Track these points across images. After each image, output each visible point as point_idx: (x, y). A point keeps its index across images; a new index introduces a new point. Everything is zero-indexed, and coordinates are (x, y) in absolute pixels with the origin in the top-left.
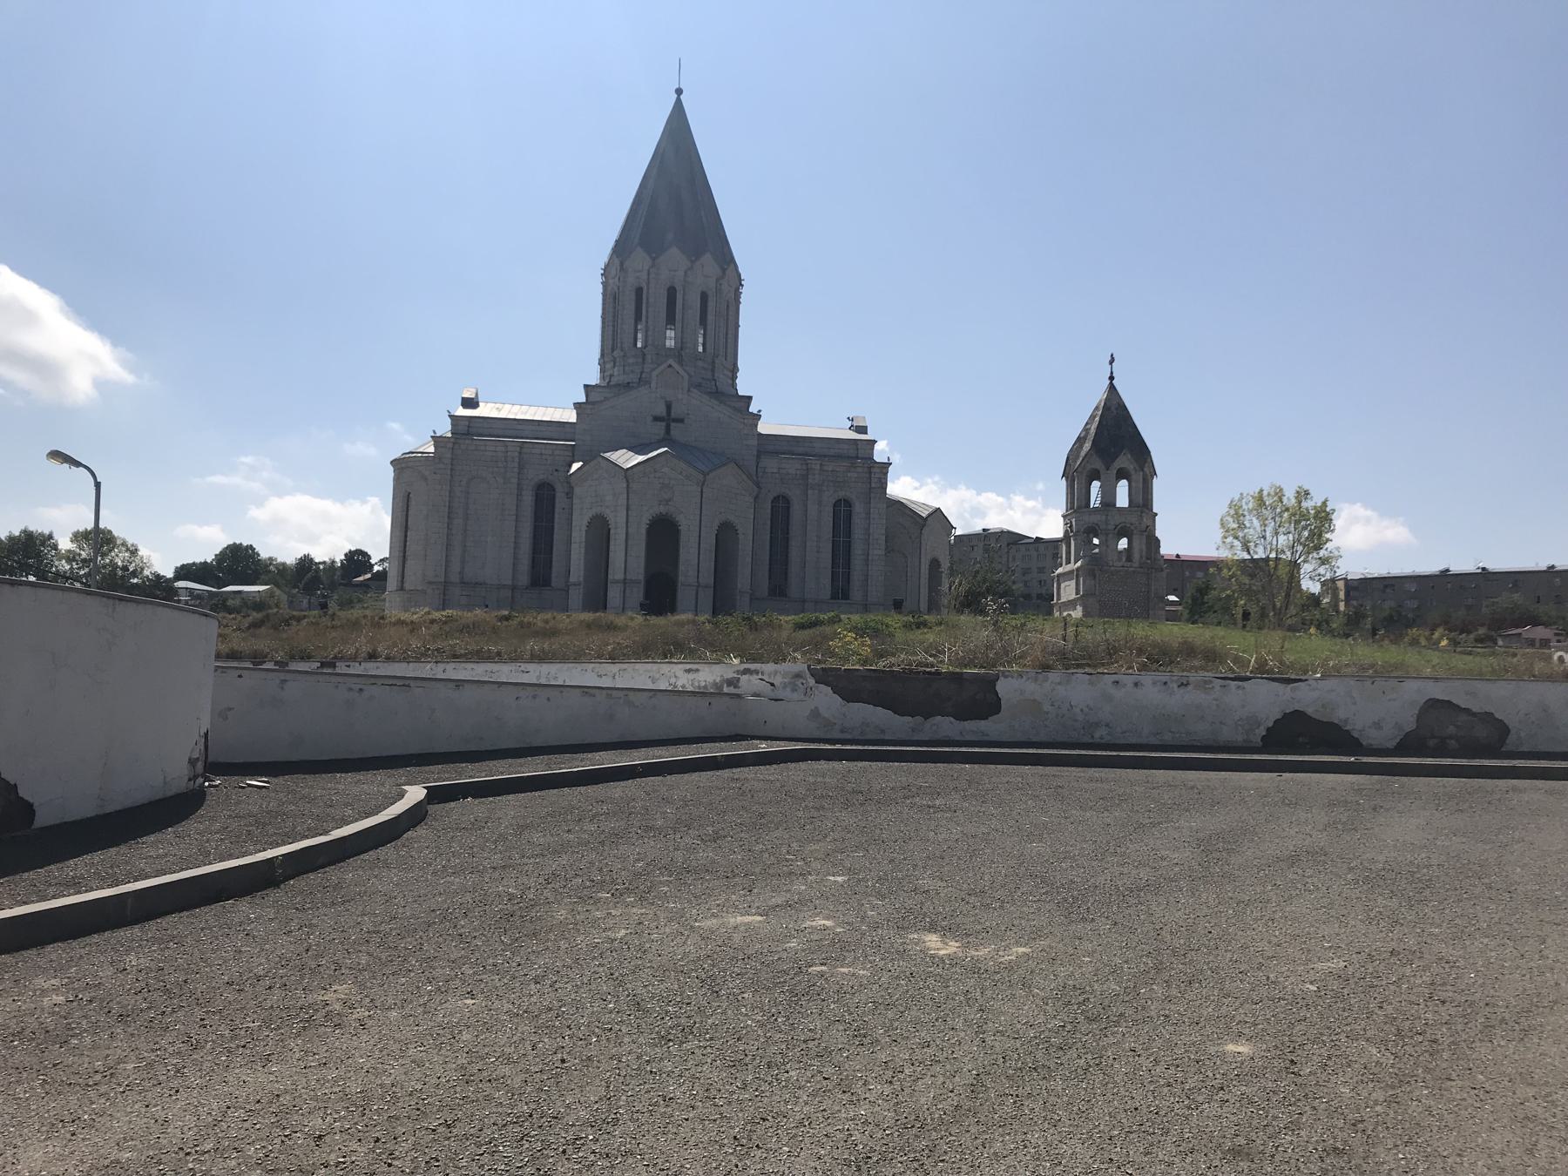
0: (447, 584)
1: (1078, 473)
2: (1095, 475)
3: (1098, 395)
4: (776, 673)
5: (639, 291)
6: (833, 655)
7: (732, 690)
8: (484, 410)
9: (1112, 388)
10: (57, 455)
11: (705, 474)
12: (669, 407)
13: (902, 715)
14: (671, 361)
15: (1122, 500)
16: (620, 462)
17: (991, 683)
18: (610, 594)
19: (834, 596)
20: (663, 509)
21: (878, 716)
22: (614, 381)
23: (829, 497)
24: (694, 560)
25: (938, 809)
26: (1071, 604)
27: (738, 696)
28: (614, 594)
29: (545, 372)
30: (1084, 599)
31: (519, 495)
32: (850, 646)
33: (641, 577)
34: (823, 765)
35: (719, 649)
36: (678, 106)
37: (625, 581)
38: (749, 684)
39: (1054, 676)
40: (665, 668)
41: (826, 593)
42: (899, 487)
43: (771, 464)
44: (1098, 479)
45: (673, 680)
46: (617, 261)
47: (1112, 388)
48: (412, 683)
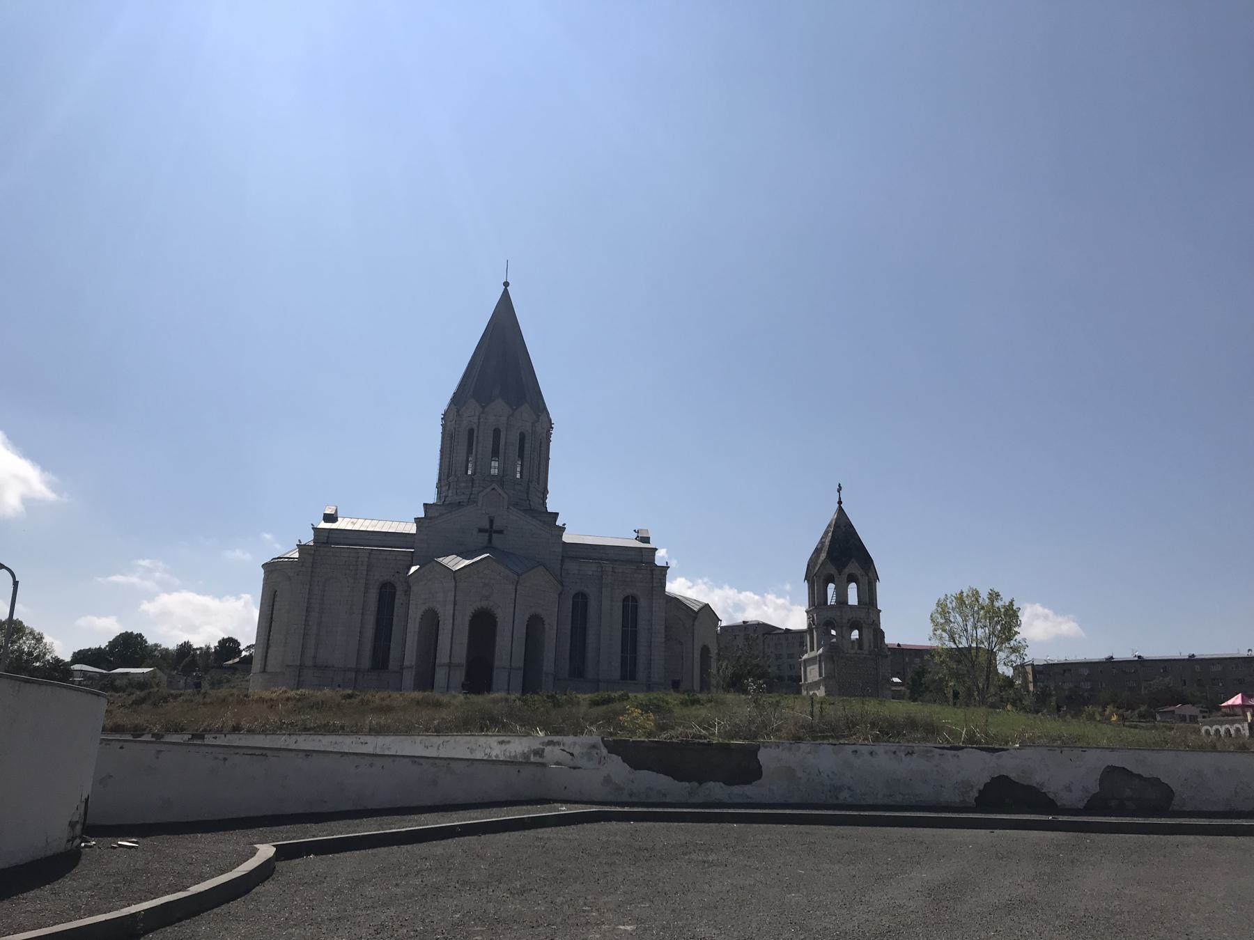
0: (302, 667)
1: (817, 577)
2: (830, 579)
3: (830, 515)
4: (575, 744)
5: (471, 432)
6: (623, 728)
7: (537, 759)
8: (341, 524)
9: (840, 510)
12: (491, 521)
13: (680, 779)
15: (853, 599)
16: (450, 566)
17: (752, 752)
18: (437, 676)
19: (624, 677)
20: (484, 604)
22: (448, 500)
24: (508, 646)
25: (711, 864)
26: (816, 685)
27: (543, 765)
28: (440, 676)
29: (391, 495)
30: (826, 680)
32: (637, 721)
33: (464, 661)
34: (614, 825)
35: (528, 724)
36: (506, 295)
37: (450, 665)
38: (553, 753)
39: (805, 747)
40: (482, 740)
41: (617, 674)
42: (676, 586)
45: (488, 751)
47: (840, 510)
48: (269, 753)
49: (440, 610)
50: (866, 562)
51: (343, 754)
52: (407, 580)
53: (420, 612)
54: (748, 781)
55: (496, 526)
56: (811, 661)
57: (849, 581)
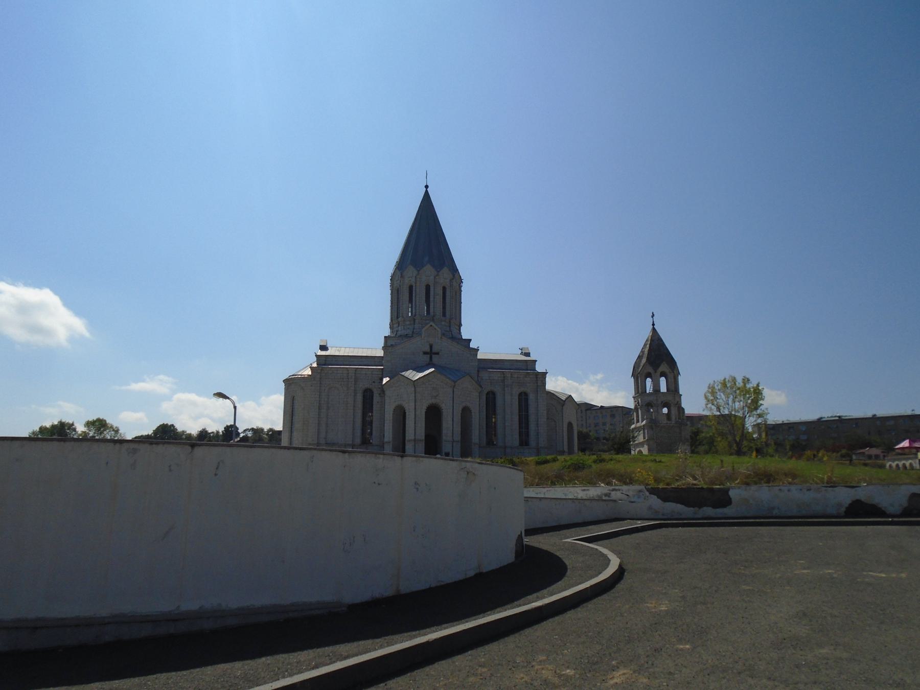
0: (318, 444)
1: (639, 375)
2: (649, 375)
3: (647, 333)
5: (411, 288)
7: (607, 498)
9: (654, 330)
10: (221, 395)
11: (455, 382)
12: (431, 347)
14: (432, 323)
15: (663, 389)
17: (726, 491)
18: (407, 447)
20: (433, 401)
21: (679, 508)
22: (399, 333)
23: (516, 391)
24: (450, 427)
26: (642, 444)
27: (615, 501)
28: (409, 447)
30: (648, 442)
31: (355, 396)
40: (572, 489)
42: (553, 384)
43: (484, 375)
44: (651, 377)
46: (399, 273)
47: (654, 330)
49: (406, 406)
50: (672, 363)
51: (541, 499)
52: (382, 389)
53: (393, 407)
54: (724, 506)
55: (434, 350)
56: (638, 429)
57: (661, 376)
